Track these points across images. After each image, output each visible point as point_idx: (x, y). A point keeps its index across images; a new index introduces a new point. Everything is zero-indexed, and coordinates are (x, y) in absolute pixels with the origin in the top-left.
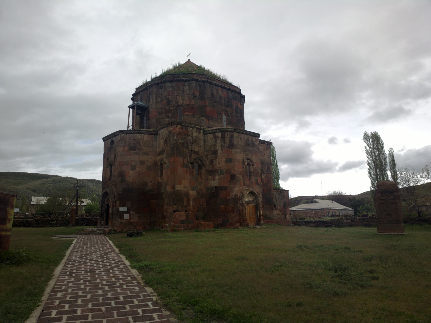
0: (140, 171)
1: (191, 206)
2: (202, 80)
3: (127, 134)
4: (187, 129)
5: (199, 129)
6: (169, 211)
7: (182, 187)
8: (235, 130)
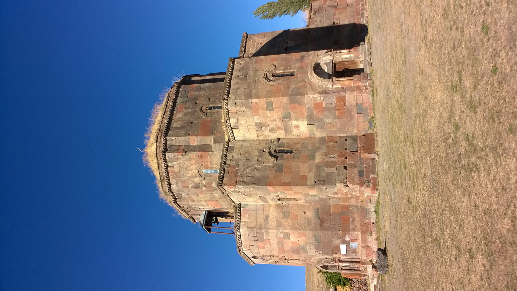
1: (338, 160)
2: (164, 143)
3: (242, 243)
4: (228, 167)
5: (227, 148)
6: (346, 192)
7: (310, 174)
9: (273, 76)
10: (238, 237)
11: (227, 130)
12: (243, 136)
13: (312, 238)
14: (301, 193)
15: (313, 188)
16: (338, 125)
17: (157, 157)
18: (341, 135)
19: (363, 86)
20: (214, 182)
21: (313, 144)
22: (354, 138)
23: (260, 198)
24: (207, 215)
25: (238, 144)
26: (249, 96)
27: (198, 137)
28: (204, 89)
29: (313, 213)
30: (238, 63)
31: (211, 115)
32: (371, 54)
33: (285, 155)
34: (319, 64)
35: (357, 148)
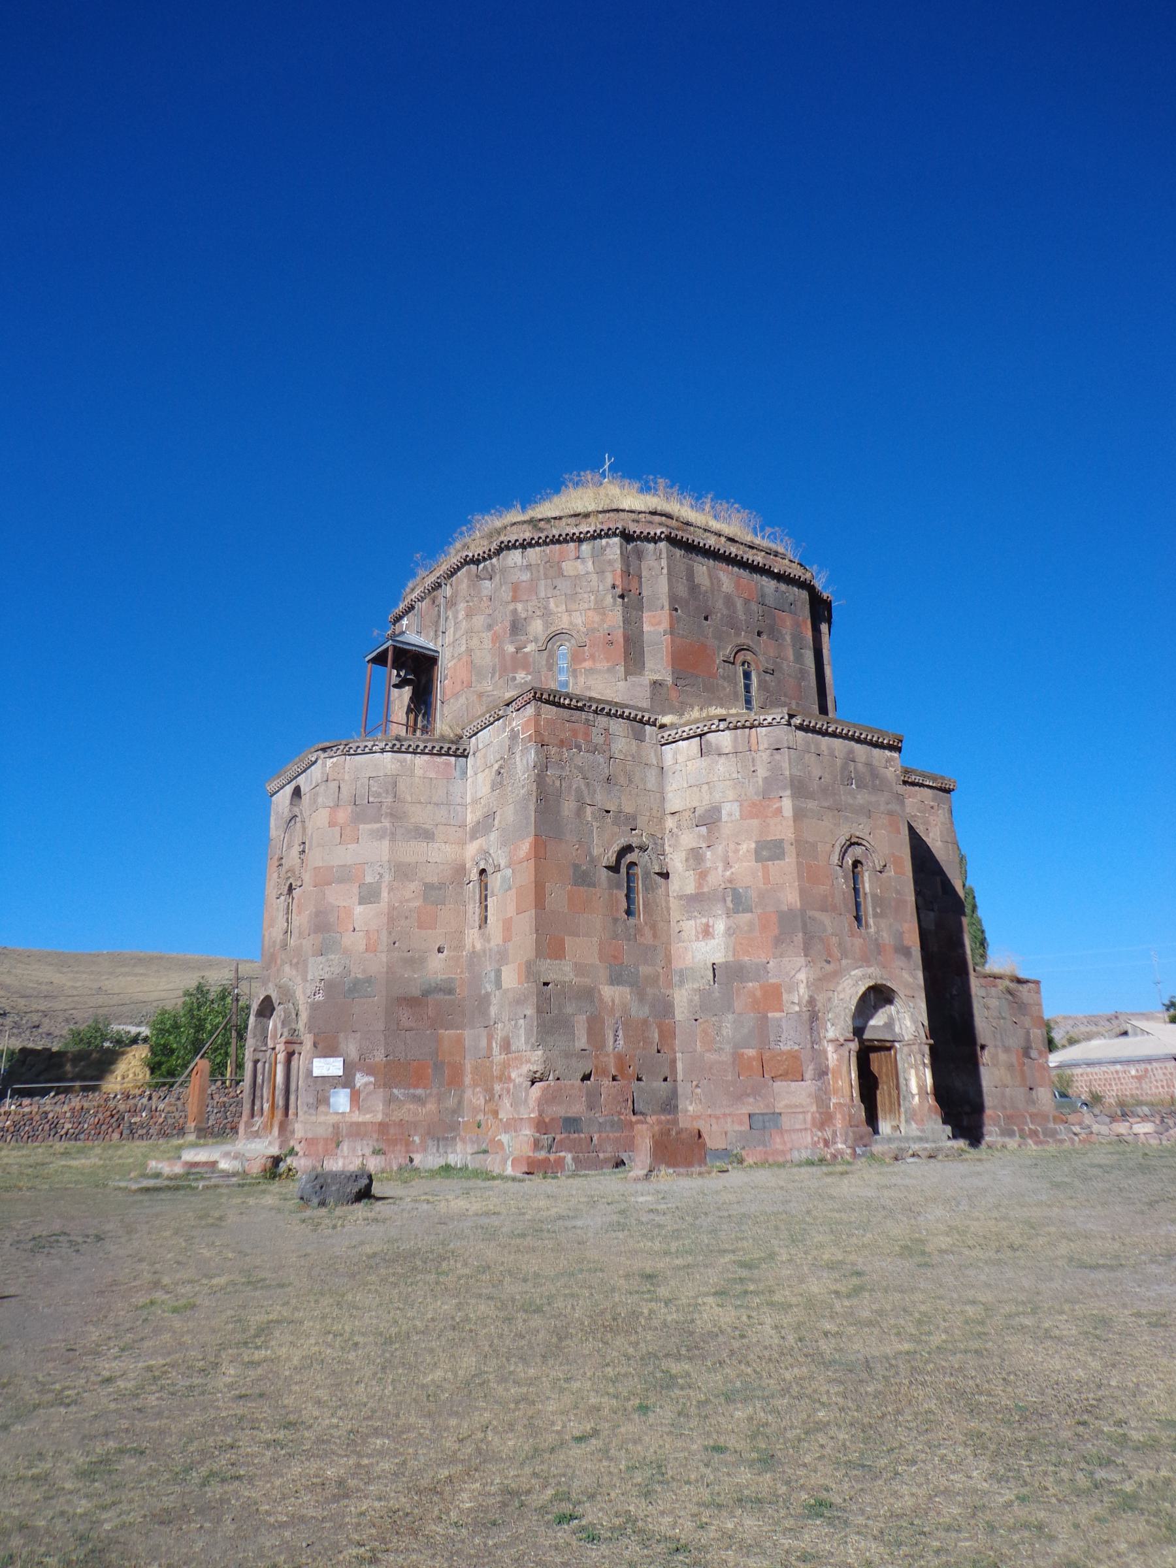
0: (396, 905)
1: (608, 1055)
2: (649, 533)
4: (587, 720)
6: (513, 1075)
7: (567, 969)
9: (856, 863)
10: (366, 746)
11: (696, 721)
12: (678, 767)
13: (364, 971)
14: (507, 939)
15: (527, 977)
16: (711, 1057)
17: (609, 511)
18: (679, 1066)
19: (834, 1133)
21: (654, 980)
22: (669, 1105)
23: (490, 816)
25: (652, 754)
26: (800, 789)
27: (668, 636)
28: (799, 658)
30: (889, 760)
31: (728, 676)
32: (931, 1157)
34: (890, 1001)
35: (642, 1114)
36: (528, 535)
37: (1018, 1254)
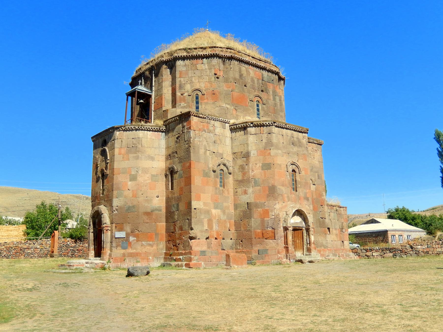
0: (142, 182)
1: (214, 231)
2: (227, 56)
7: (202, 204)
8: (274, 123)
13: (132, 203)
20: (186, 104)
24: (147, 94)
25: (228, 133)
28: (274, 99)
29: (157, 205)
31: (252, 106)
33: (218, 180)
36: (185, 54)
37: (343, 282)
